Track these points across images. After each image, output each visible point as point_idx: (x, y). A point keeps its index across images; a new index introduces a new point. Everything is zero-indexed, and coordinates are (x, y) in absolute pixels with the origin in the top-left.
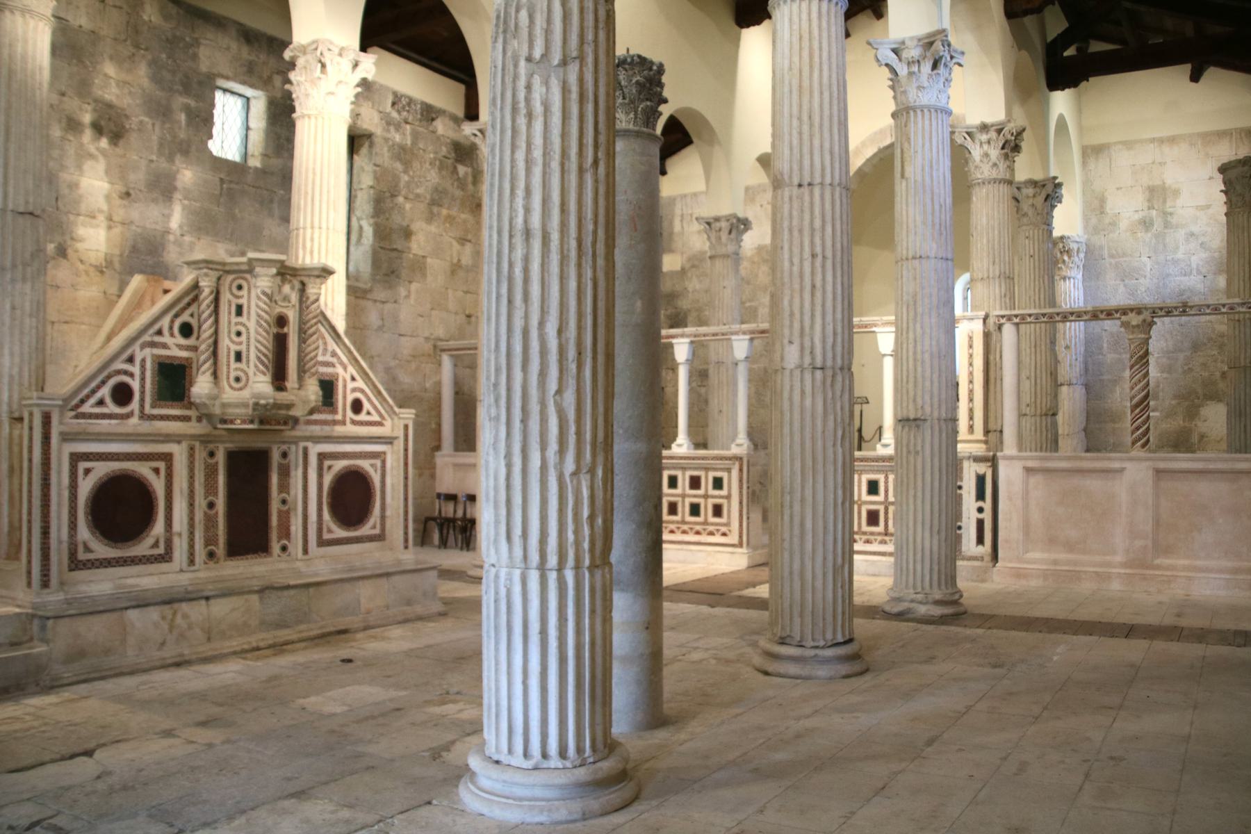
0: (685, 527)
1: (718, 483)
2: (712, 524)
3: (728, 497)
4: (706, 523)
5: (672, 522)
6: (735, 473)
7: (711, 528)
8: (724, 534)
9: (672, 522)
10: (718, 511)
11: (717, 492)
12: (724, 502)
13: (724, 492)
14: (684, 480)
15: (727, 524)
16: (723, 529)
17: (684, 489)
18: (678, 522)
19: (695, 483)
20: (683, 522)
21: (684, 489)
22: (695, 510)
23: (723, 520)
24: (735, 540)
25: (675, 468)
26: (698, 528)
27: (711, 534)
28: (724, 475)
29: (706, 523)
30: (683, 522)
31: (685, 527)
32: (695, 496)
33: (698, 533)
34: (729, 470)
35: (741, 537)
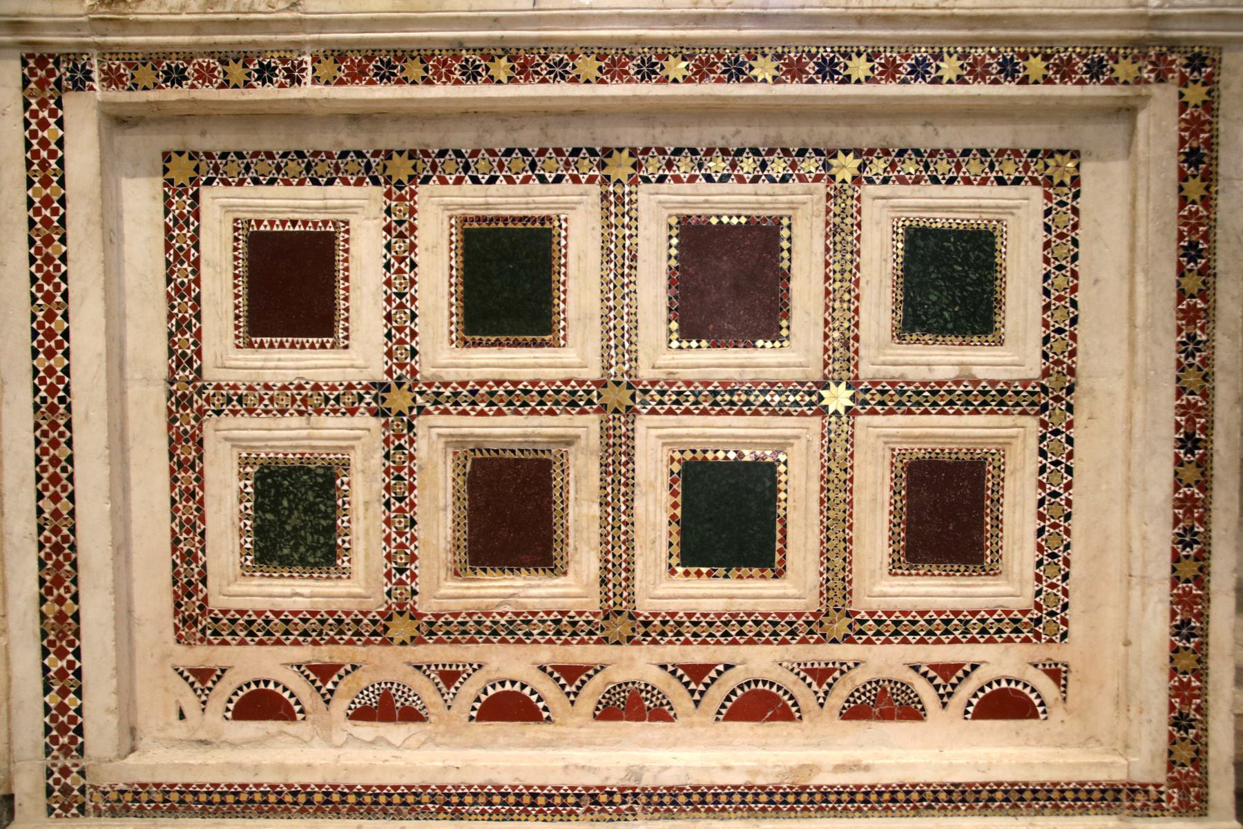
0: (640, 665)
1: (949, 283)
2: (898, 627)
3: (1050, 397)
4: (835, 617)
5: (514, 628)
6: (1125, 200)
7: (886, 661)
8: (1005, 704)
9: (514, 628)
10: (945, 513)
11: (940, 360)
12: (1015, 438)
13: (1014, 355)
14: (620, 261)
15: (1043, 621)
16: (1000, 662)
17: (619, 333)
18: (564, 626)
19: (729, 282)
20: (619, 620)
21: (619, 333)
22: (728, 516)
23: (1010, 585)
24: (1143, 760)
25: (530, 163)
26: (761, 662)
27: (886, 704)
28: (1019, 218)
29: (835, 617)
30: (619, 620)
31: (640, 665)
32: (721, 398)
33: (759, 705)
34: (1052, 172)
35: (1186, 718)
